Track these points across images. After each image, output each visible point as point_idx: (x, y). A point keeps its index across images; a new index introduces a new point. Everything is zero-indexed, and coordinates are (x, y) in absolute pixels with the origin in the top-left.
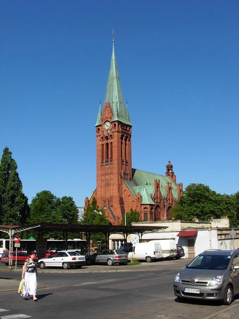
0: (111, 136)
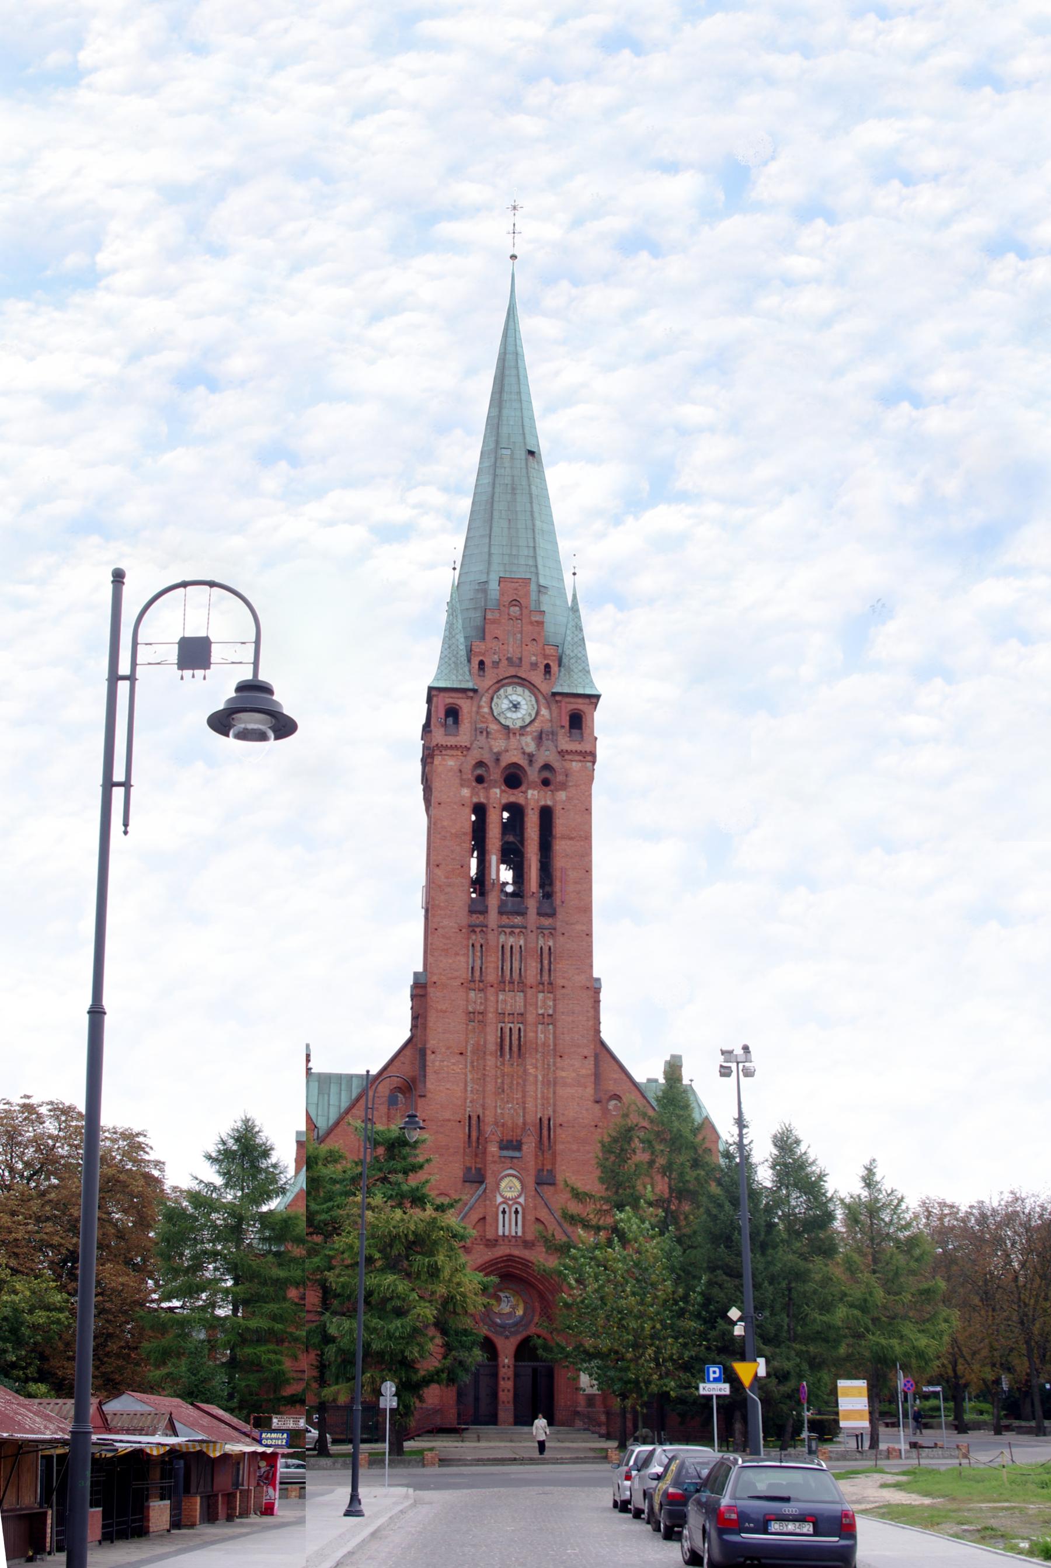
0: (547, 767)
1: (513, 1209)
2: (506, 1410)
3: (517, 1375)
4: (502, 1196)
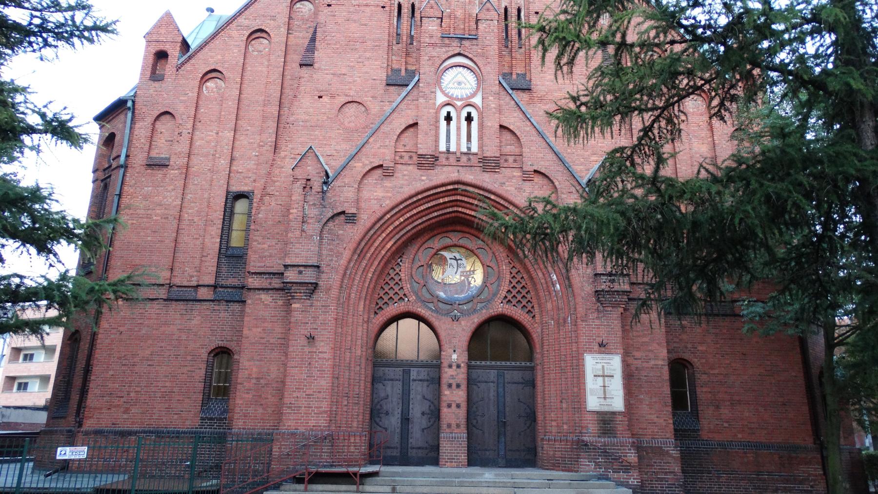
1: (464, 114)
2: (454, 443)
3: (471, 382)
4: (446, 95)
